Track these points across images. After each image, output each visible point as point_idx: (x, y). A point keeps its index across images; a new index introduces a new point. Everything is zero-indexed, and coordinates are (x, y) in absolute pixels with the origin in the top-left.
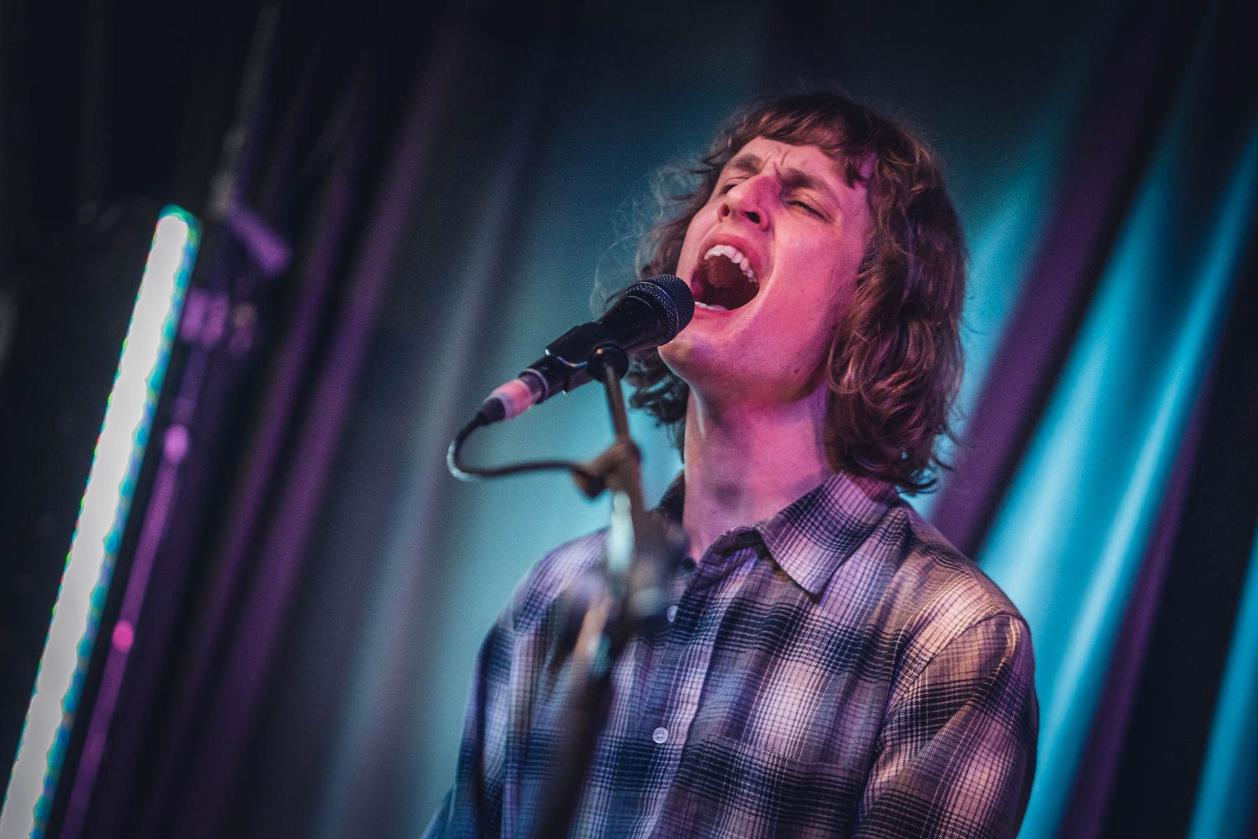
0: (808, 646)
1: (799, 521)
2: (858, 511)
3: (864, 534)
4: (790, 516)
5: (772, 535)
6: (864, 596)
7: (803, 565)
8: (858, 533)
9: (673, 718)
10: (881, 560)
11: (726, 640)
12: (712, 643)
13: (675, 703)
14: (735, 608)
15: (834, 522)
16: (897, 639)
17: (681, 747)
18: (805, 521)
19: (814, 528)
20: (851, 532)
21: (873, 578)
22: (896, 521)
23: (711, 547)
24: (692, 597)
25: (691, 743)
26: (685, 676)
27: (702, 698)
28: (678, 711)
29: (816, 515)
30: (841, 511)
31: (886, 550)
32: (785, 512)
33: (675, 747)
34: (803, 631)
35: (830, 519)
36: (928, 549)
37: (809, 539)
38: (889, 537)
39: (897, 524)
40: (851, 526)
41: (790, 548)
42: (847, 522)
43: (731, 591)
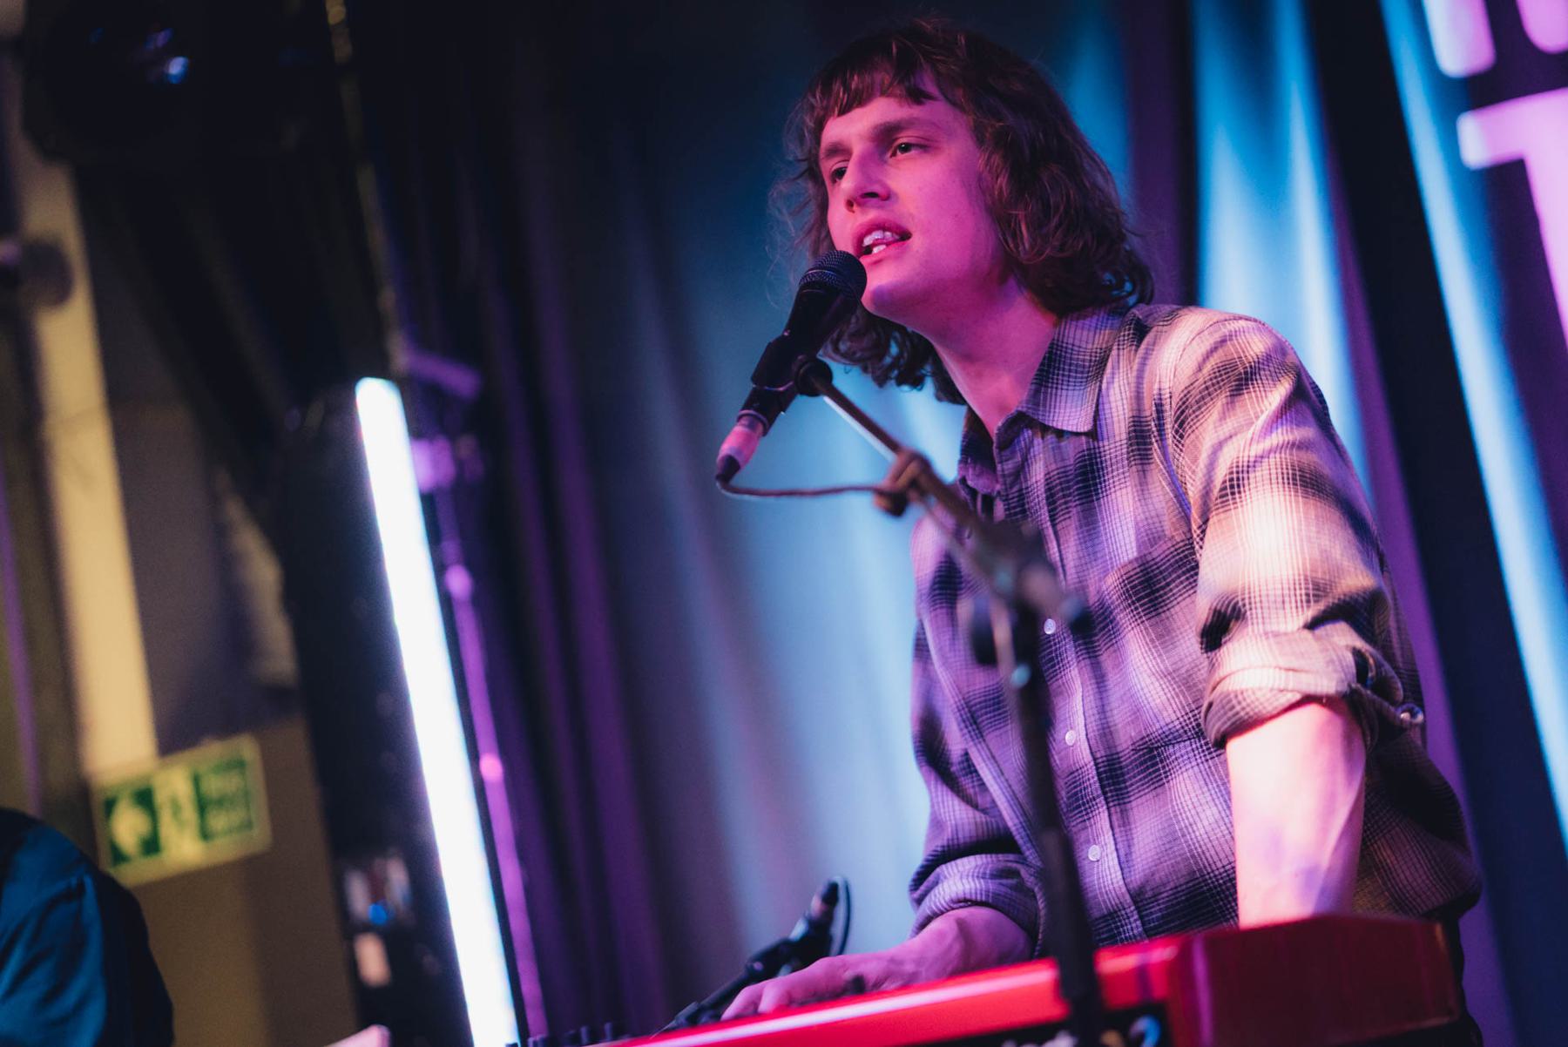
0: (1115, 473)
1: (1050, 380)
5: (1035, 407)
19: (1066, 378)
29: (1062, 366)
30: (1081, 350)
32: (1035, 381)
37: (1067, 390)
40: (1096, 357)
41: (1055, 408)
42: (1091, 356)
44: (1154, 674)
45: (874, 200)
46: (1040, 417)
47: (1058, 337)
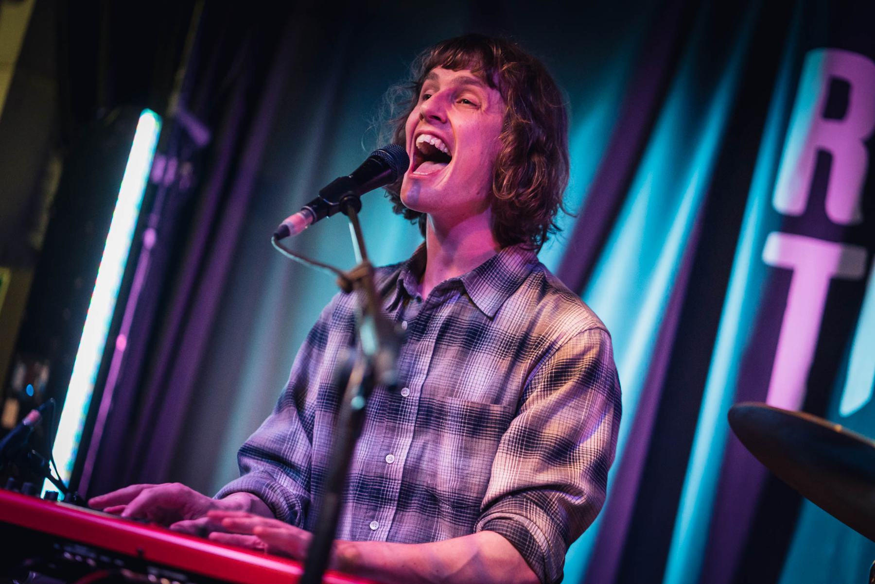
1: (484, 275)
2: (516, 270)
3: (519, 283)
4: (479, 272)
6: (520, 317)
7: (485, 300)
8: (516, 282)
9: (413, 381)
10: (529, 298)
11: (442, 339)
12: (434, 341)
13: (414, 374)
14: (447, 321)
15: (503, 275)
16: (538, 339)
17: (418, 398)
18: (487, 275)
19: (491, 279)
20: (513, 281)
21: (525, 307)
22: (537, 276)
23: (435, 288)
24: (424, 314)
25: (423, 396)
26: (419, 358)
27: (429, 371)
28: (415, 377)
29: (493, 271)
30: (507, 269)
31: (532, 292)
32: (477, 270)
33: (414, 398)
34: (487, 336)
35: (501, 274)
36: (557, 291)
37: (489, 285)
38: (534, 285)
39: (538, 277)
40: (512, 278)
41: (478, 290)
42: (510, 276)
43: (445, 312)
44: (451, 463)
45: (437, 121)
46: (469, 290)
47: (500, 256)
